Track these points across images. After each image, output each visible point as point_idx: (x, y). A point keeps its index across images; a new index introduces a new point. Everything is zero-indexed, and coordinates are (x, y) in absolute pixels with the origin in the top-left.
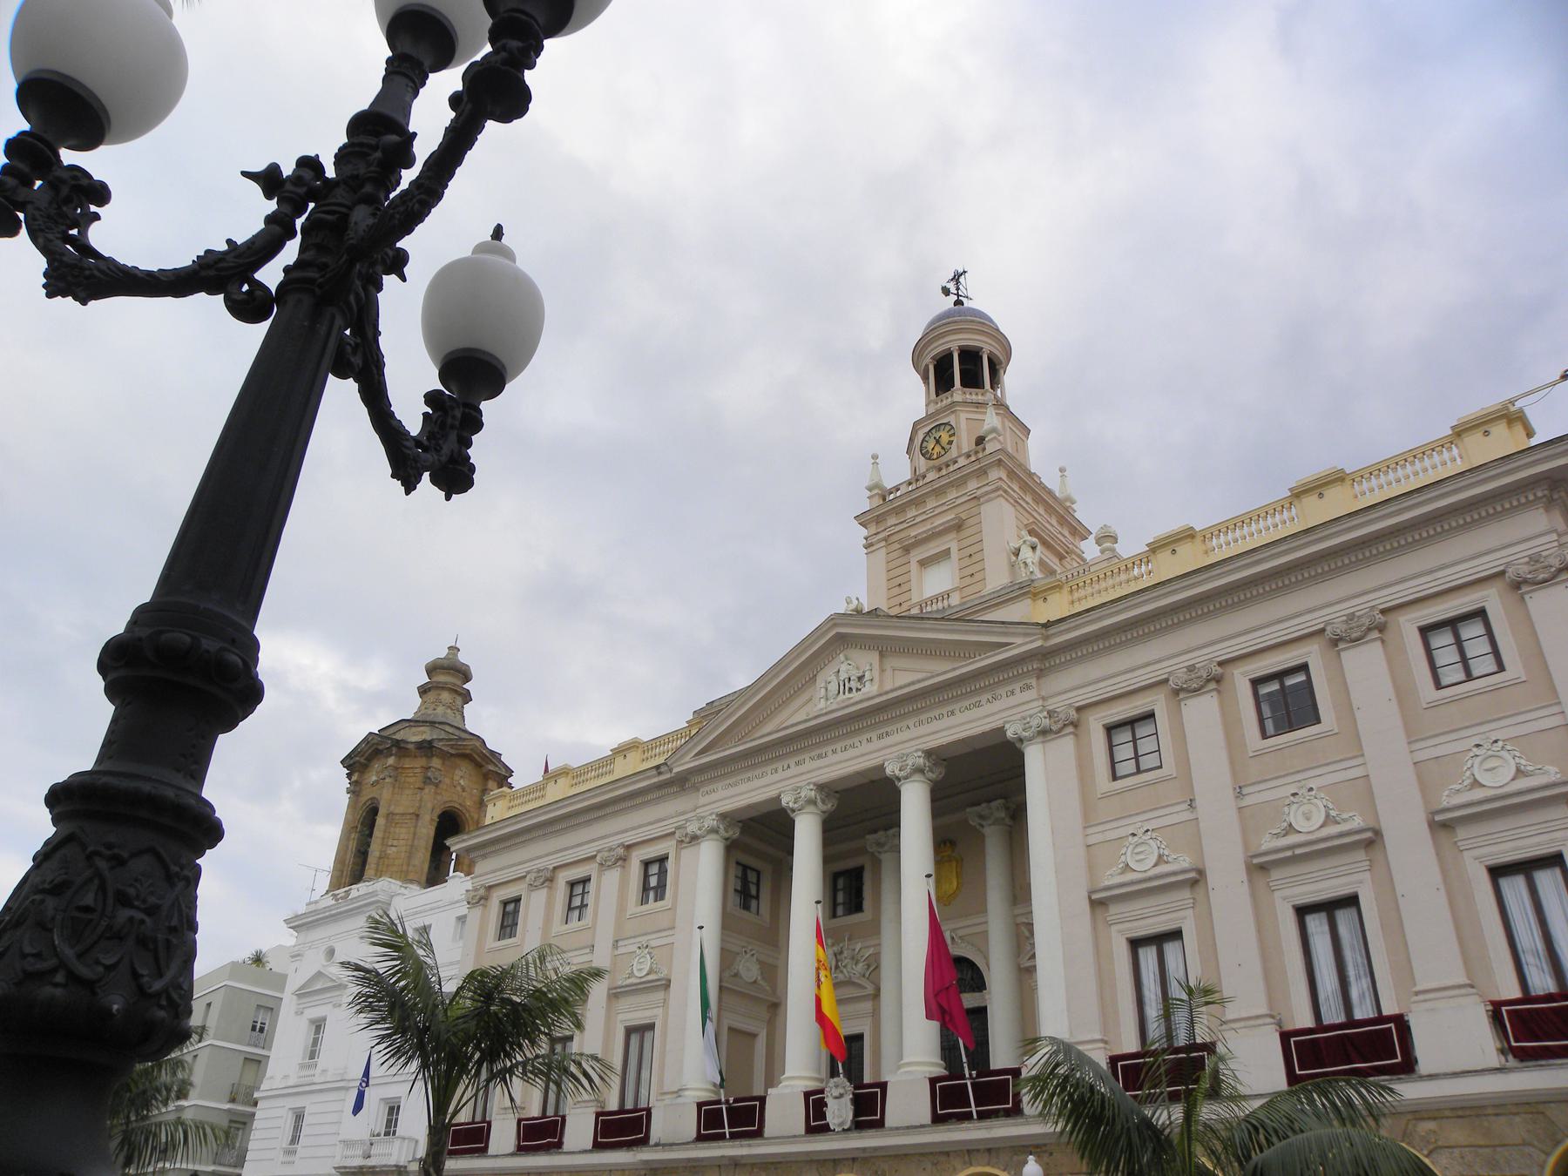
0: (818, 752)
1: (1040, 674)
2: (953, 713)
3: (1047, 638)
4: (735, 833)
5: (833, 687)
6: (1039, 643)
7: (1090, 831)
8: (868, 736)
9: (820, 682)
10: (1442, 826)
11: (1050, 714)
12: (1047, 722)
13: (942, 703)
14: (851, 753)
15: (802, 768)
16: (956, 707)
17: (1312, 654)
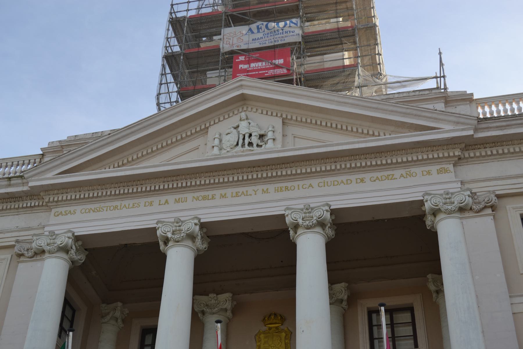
0: (206, 193)
1: (459, 161)
2: (362, 180)
3: (476, 130)
4: (81, 258)
5: (232, 138)
6: (471, 132)
7: (516, 300)
9: (213, 131)
11: (473, 195)
12: (469, 200)
13: (353, 170)
14: (242, 199)
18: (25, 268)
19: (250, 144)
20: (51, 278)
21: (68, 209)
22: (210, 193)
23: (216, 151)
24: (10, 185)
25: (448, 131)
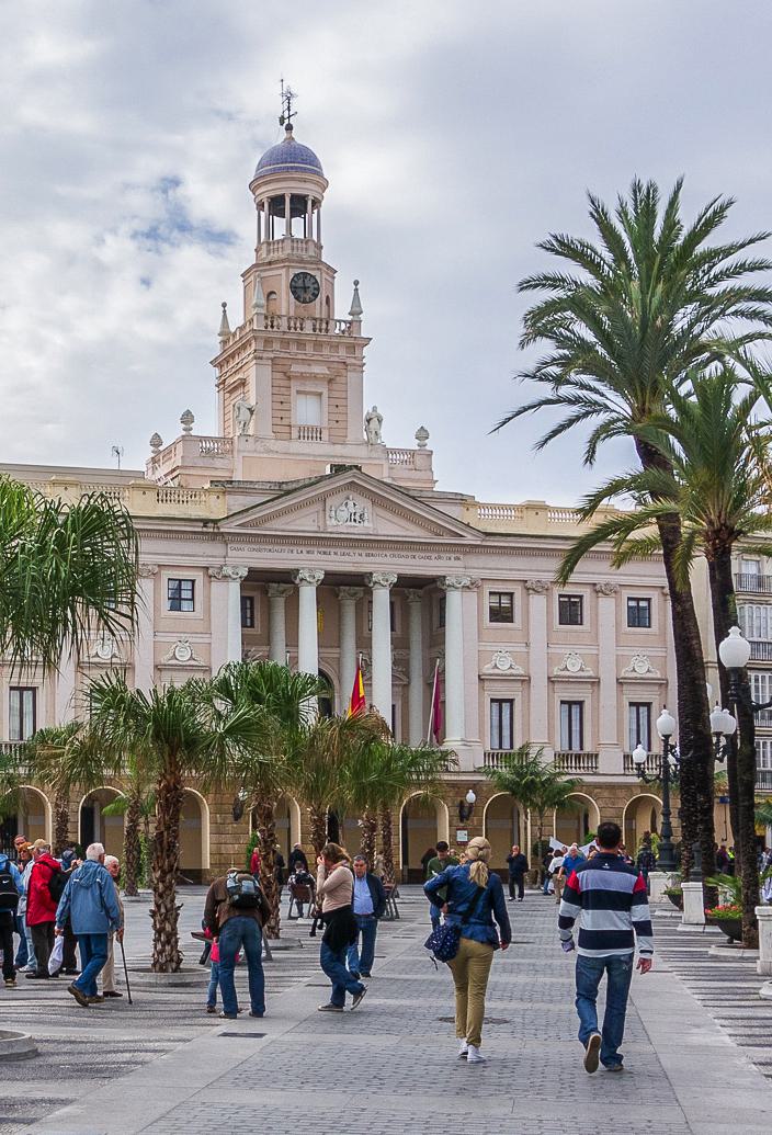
1: (465, 553)
5: (345, 515)
8: (360, 552)
10: (620, 683)
15: (310, 556)
16: (417, 554)
17: (587, 593)
18: (216, 586)
19: (355, 520)
20: (233, 591)
21: (239, 546)
22: (328, 550)
23: (334, 522)
24: (205, 526)
25: (470, 539)
